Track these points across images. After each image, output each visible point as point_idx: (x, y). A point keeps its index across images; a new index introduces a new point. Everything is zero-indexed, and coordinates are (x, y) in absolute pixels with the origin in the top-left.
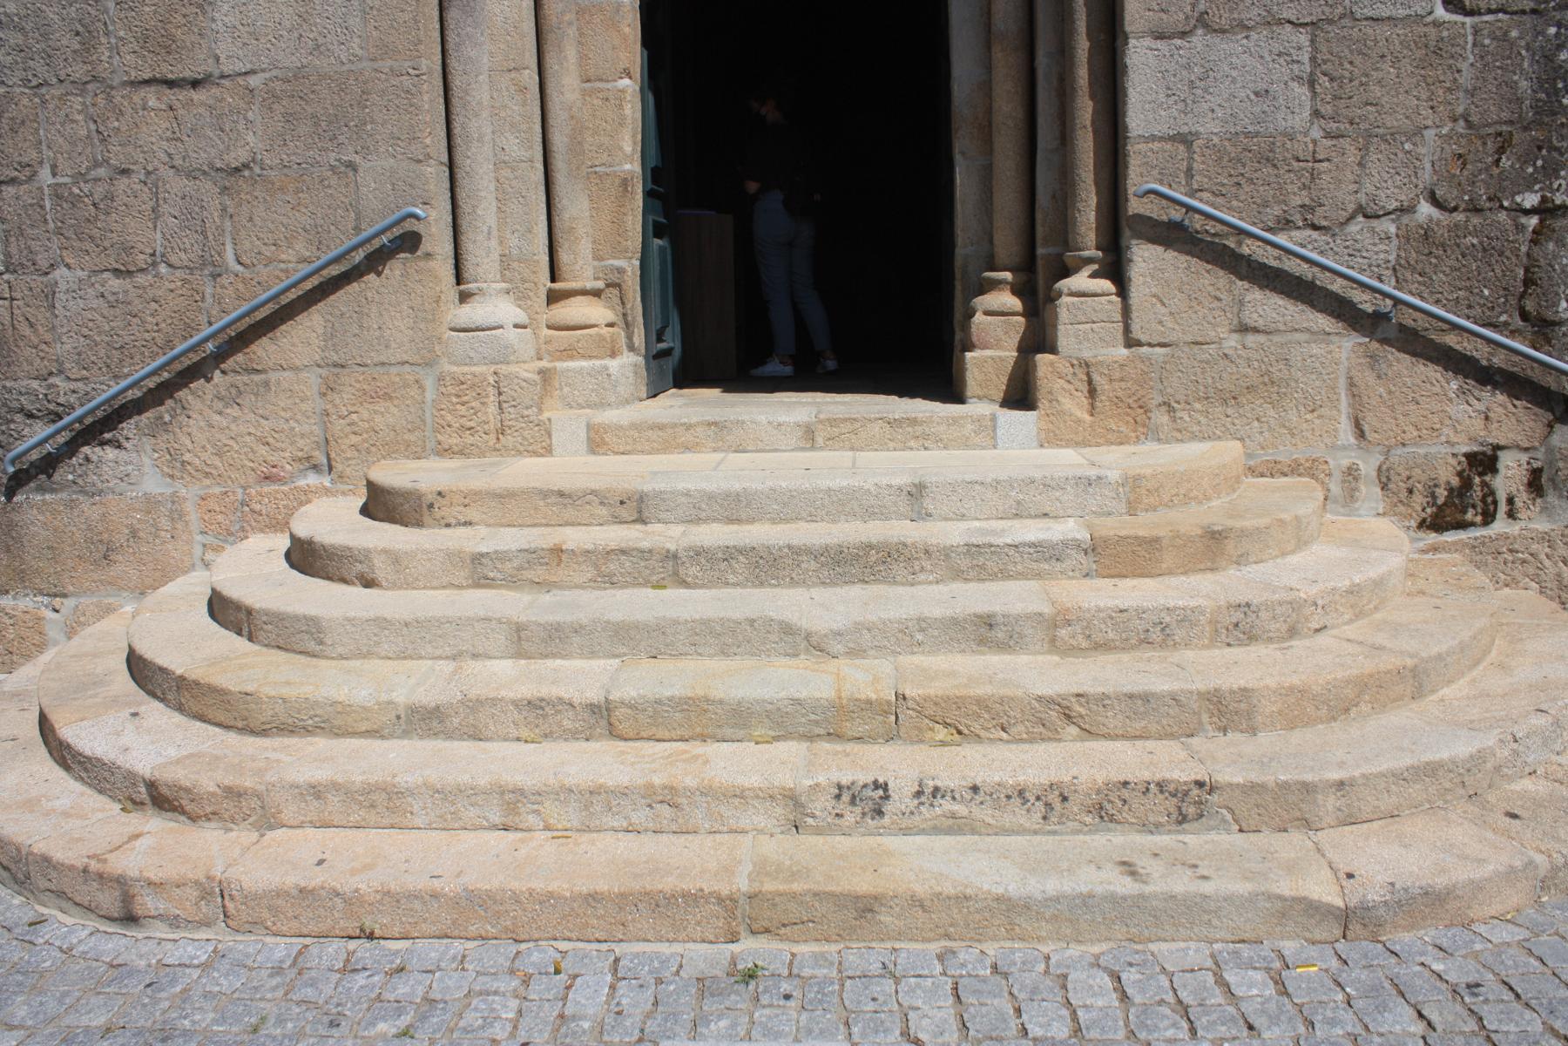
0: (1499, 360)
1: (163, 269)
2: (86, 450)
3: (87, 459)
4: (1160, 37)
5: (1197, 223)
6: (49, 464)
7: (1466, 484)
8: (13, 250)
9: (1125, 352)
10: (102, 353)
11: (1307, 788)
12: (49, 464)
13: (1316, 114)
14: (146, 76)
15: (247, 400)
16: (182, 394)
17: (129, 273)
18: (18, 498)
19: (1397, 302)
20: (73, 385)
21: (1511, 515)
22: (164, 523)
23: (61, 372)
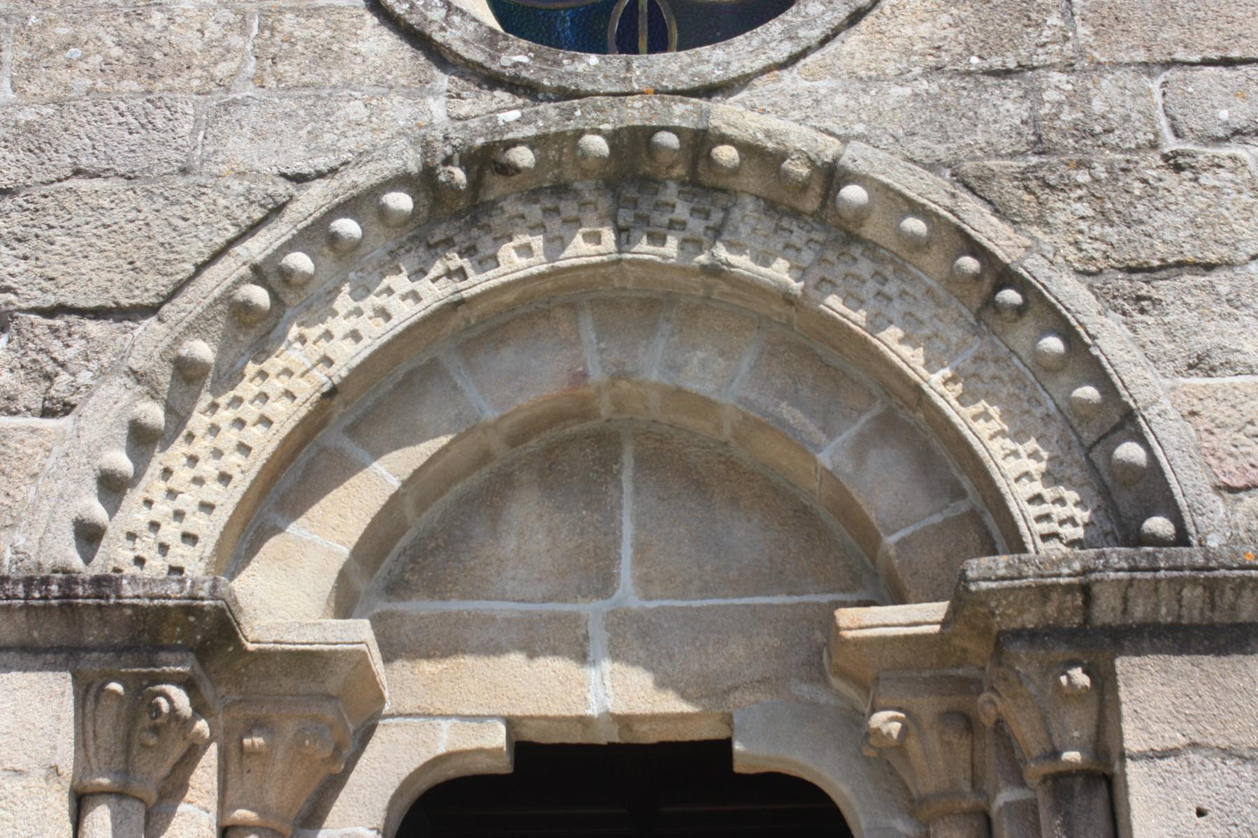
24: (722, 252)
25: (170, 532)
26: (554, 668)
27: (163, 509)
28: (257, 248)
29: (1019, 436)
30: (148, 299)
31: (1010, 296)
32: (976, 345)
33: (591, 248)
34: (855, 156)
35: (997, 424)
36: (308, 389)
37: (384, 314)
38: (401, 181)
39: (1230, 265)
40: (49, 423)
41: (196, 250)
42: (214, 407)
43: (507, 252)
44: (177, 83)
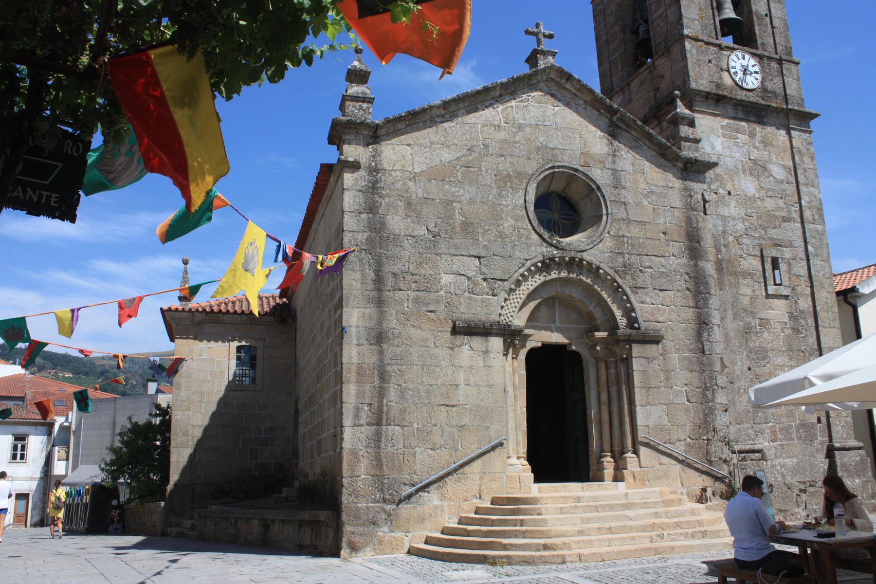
0: (704, 469)
1: (443, 449)
2: (420, 493)
3: (420, 496)
4: (642, 406)
5: (651, 443)
6: (409, 497)
7: (702, 494)
8: (406, 442)
9: (639, 469)
10: (427, 468)
11: (719, 531)
12: (409, 497)
13: (669, 421)
14: (442, 403)
15: (462, 481)
16: (446, 479)
17: (435, 449)
18: (400, 506)
19: (686, 458)
20: (418, 477)
21: (710, 501)
22: (439, 512)
23: (415, 473)
24: (582, 277)
25: (509, 315)
26: (548, 333)
27: (507, 311)
28: (521, 271)
29: (619, 310)
30: (507, 278)
31: (620, 290)
32: (614, 295)
33: (564, 274)
34: (602, 265)
35: (616, 308)
36: (526, 292)
37: (536, 282)
38: (540, 262)
39: (646, 288)
40: (494, 298)
41: (513, 271)
42: (513, 295)
43: (552, 273)
44: (507, 240)
